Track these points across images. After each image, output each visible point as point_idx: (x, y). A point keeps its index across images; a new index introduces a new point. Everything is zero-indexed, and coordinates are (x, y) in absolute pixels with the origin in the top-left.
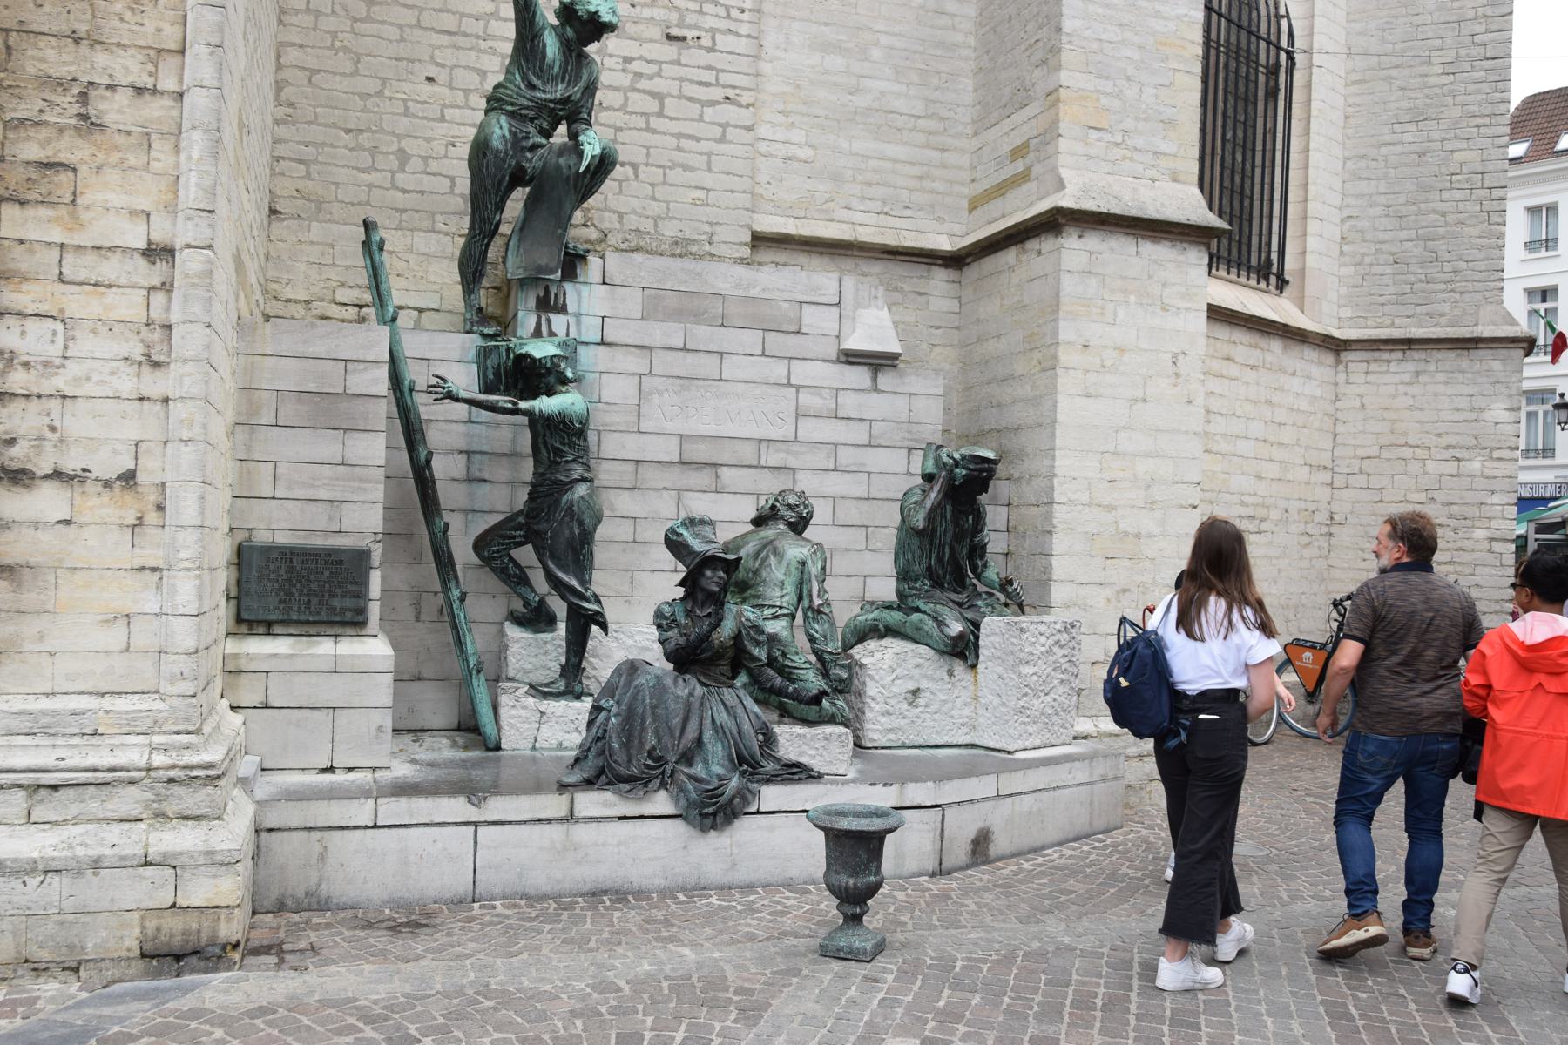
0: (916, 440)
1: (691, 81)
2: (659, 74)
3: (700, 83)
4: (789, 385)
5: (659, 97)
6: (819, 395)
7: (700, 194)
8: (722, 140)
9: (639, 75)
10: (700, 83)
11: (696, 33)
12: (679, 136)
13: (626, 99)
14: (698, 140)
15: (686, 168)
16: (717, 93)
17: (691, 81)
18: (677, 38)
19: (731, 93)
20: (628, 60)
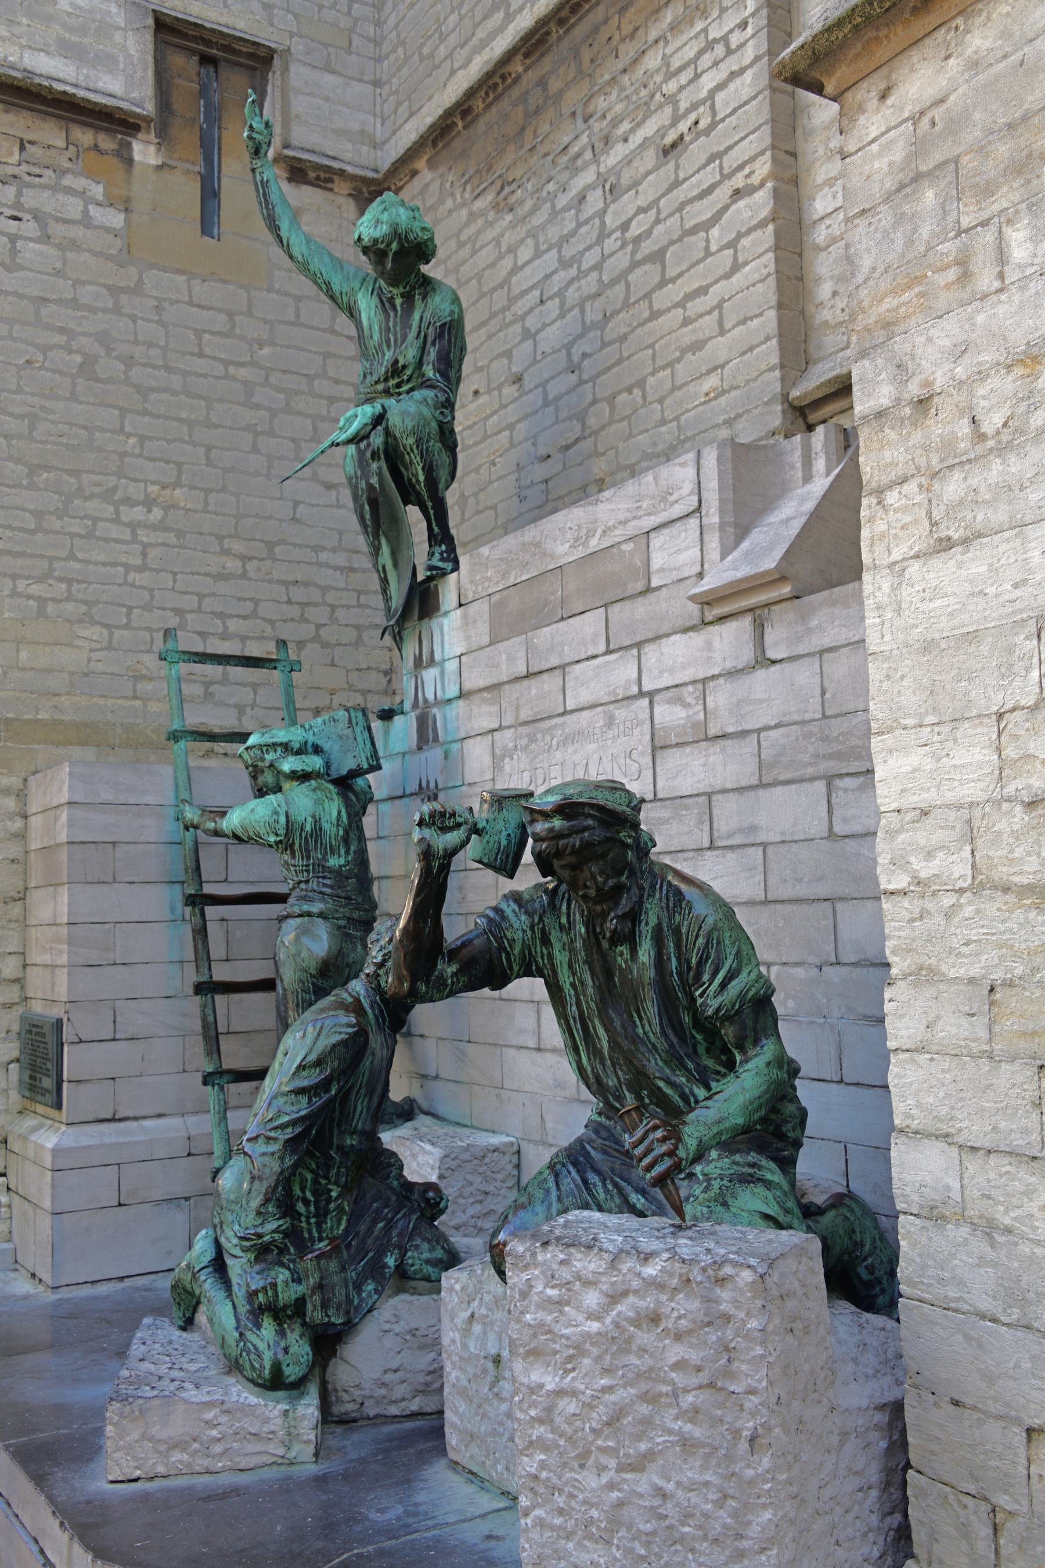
0: (837, 756)
1: (691, 201)
2: (658, 221)
3: (701, 196)
4: (641, 694)
5: (658, 257)
6: (680, 701)
7: (712, 382)
8: (736, 267)
9: (638, 240)
10: (701, 196)
11: (692, 117)
12: (681, 304)
13: (628, 285)
14: (703, 291)
15: (697, 346)
16: (722, 194)
17: (691, 201)
18: (674, 145)
19: (739, 181)
20: (625, 227)
